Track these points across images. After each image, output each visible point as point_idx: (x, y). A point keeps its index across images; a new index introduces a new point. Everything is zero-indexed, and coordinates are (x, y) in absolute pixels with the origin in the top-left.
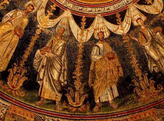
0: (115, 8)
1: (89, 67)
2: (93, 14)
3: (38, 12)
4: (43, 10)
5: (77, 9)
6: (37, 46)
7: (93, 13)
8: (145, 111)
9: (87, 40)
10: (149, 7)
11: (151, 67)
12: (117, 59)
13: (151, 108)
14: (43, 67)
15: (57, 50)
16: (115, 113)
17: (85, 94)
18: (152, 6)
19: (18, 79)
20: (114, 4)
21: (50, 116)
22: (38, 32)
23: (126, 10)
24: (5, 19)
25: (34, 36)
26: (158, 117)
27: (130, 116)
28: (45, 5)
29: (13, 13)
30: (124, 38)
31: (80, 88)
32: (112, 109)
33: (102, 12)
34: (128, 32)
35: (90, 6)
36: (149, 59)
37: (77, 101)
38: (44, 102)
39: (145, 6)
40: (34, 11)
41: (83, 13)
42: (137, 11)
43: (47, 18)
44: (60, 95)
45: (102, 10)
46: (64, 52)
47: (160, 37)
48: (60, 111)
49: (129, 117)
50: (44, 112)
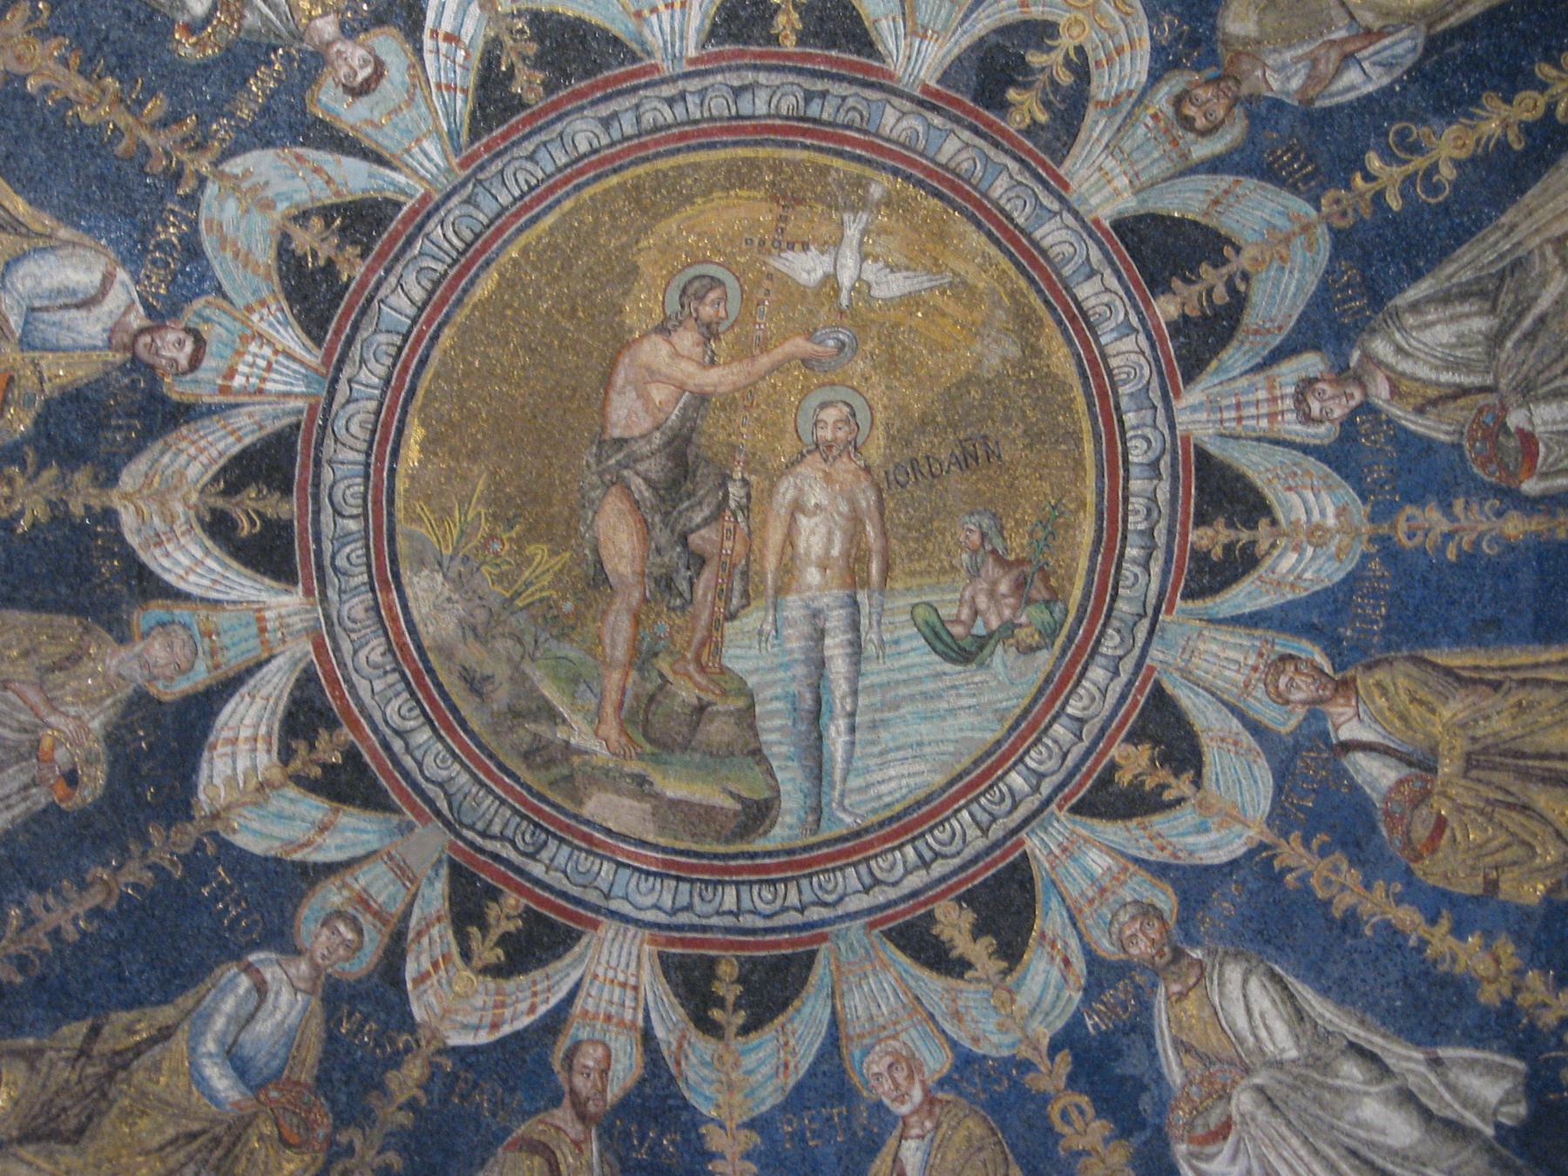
0: (561, 135)
2: (722, 70)
3: (1144, 78)
4: (1103, 86)
5: (844, 98)
7: (719, 78)
10: (303, 197)
18: (282, 206)
20: (566, 166)
24: (1399, 50)
28: (1088, 120)
29: (1334, 88)
33: (649, 92)
35: (743, 130)
39: (338, 193)
41: (791, 70)
42: (387, 141)
43: (1076, 31)
45: (656, 111)
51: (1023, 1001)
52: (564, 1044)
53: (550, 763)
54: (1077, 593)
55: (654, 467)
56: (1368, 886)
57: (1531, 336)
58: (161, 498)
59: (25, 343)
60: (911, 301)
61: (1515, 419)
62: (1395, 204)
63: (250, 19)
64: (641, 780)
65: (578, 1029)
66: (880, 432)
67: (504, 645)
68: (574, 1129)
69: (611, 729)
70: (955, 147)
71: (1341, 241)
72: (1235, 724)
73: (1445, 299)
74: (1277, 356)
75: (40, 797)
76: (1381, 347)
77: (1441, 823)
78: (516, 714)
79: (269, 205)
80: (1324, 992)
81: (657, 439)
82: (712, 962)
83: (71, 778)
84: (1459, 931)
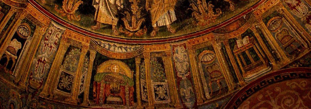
8: (204, 36)
13: (210, 33)
16: (173, 37)
17: (142, 18)
19: (74, 3)
21: (106, 41)
26: (217, 42)
27: (188, 40)
31: (137, 12)
32: (170, 33)
37: (134, 26)
38: (100, 27)
44: (116, 20)
48: (116, 35)
49: (188, 41)
50: (100, 37)
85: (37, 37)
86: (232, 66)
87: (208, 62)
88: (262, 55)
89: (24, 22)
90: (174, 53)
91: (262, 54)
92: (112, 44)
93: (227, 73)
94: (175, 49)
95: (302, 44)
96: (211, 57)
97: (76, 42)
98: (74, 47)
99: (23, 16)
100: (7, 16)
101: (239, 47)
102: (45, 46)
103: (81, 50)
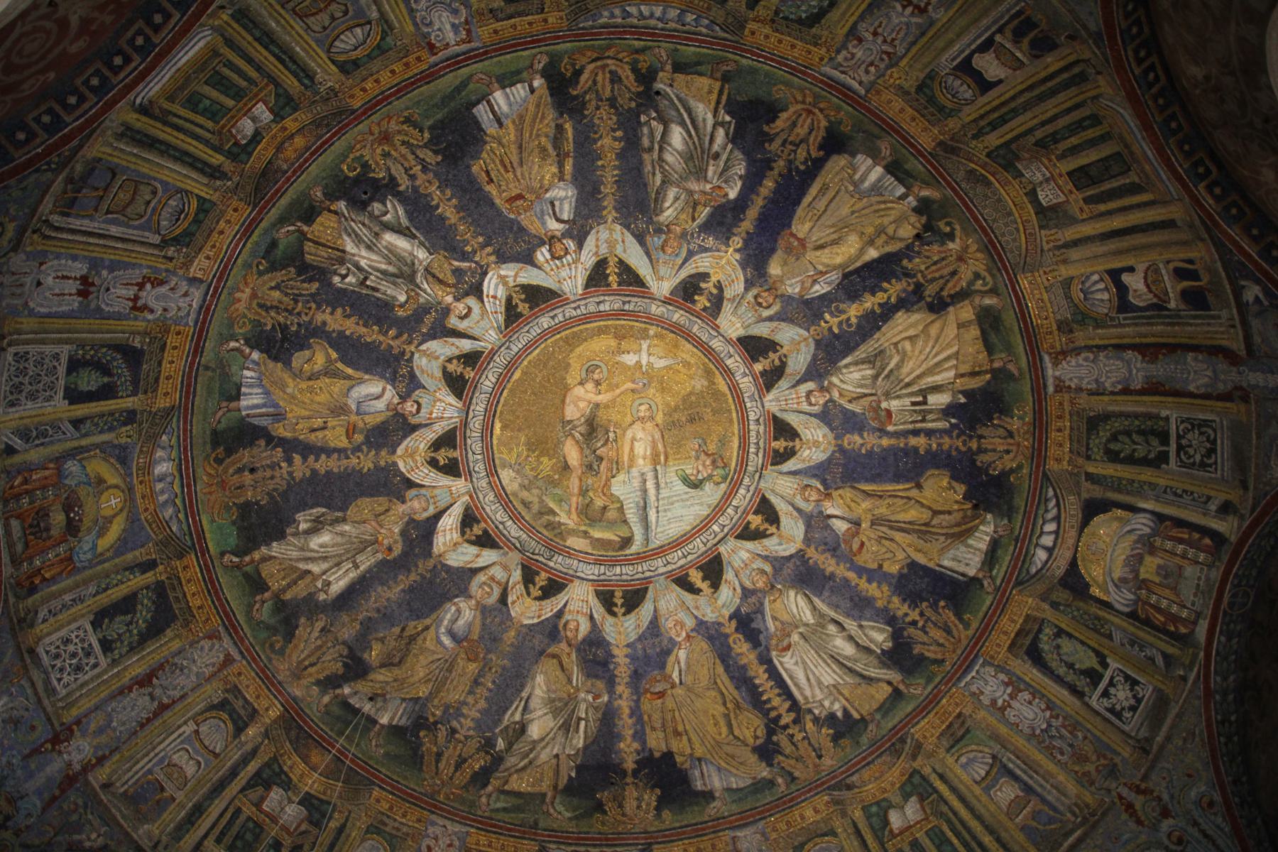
1: (574, 165)
4: (728, 294)
6: (740, 206)
9: (593, 231)
11: (394, 211)
12: (497, 201)
14: (717, 156)
15: (676, 199)
22: (737, 242)
23: (506, 327)
25: (748, 233)
27: (425, 67)
30: (493, 258)
34: (485, 274)
36: (408, 228)
37: (604, 73)
40: (754, 291)
45: (570, 312)
46: (658, 193)
47: (394, 293)
51: (720, 602)
52: (563, 621)
53: (554, 529)
54: (733, 464)
55: (582, 429)
56: (838, 564)
57: (888, 376)
58: (411, 456)
59: (358, 413)
60: (668, 368)
61: (884, 405)
62: (836, 331)
63: (422, 300)
64: (586, 532)
65: (567, 617)
66: (660, 413)
67: (535, 491)
68: (567, 650)
69: (574, 516)
70: (678, 316)
71: (818, 343)
72: (791, 508)
73: (856, 363)
74: (799, 382)
75: (380, 556)
76: (835, 380)
77: (862, 544)
78: (541, 513)
79: (437, 358)
80: (823, 601)
81: (583, 420)
82: (613, 592)
83: (390, 549)
84: (869, 581)
85: (919, 66)
86: (266, 48)
87: (350, 29)
88: (180, 117)
89: (952, 110)
90: (467, 22)
91: (181, 122)
92: (672, 25)
93: (278, 22)
94: (463, 34)
95: (68, 215)
96: (342, 46)
97: (789, 35)
98: (800, 21)
99: (953, 124)
100: (1002, 140)
101: (260, 104)
102: (893, 40)
103: (777, 13)
